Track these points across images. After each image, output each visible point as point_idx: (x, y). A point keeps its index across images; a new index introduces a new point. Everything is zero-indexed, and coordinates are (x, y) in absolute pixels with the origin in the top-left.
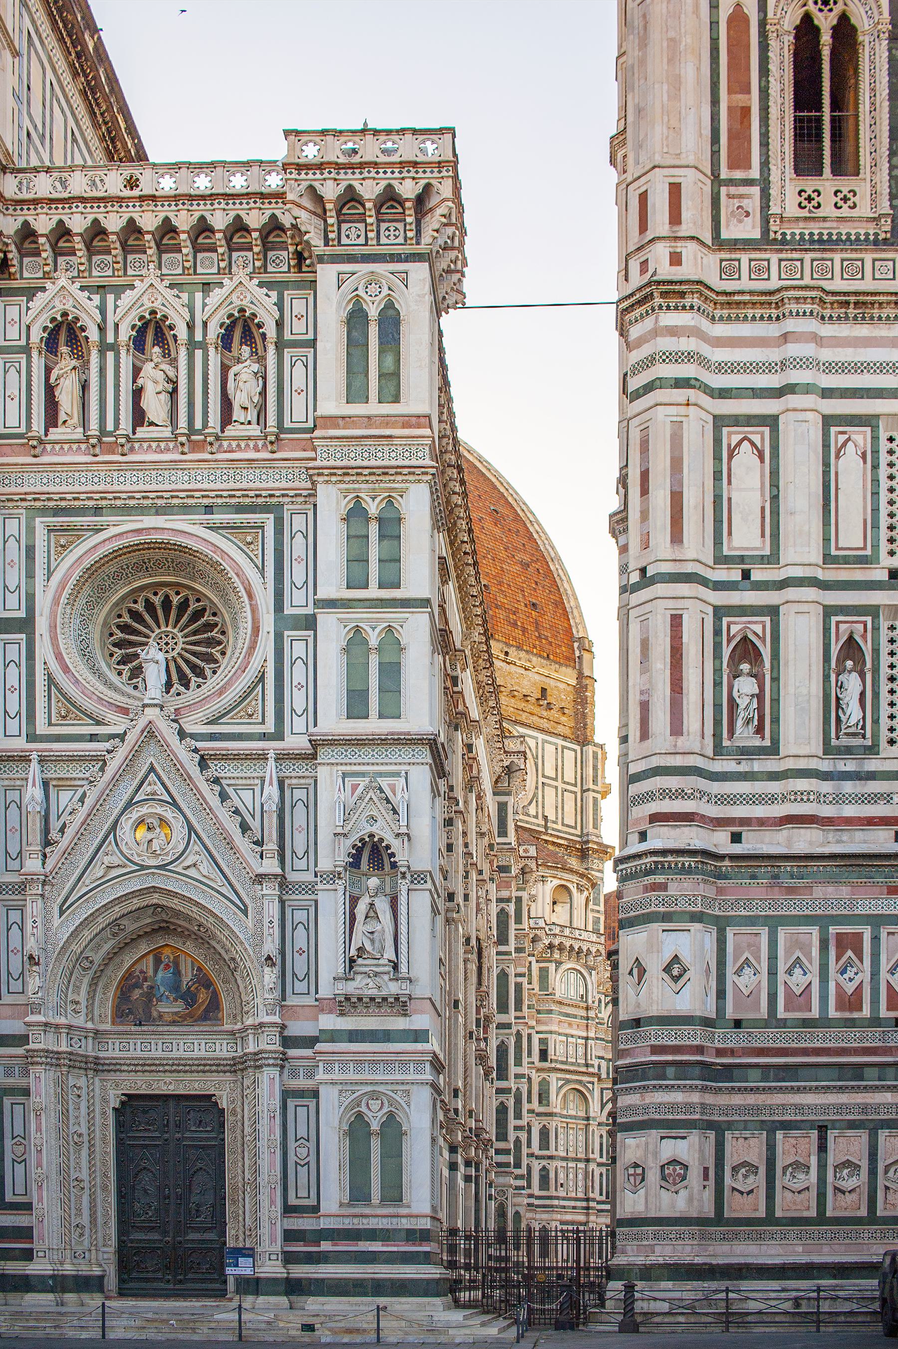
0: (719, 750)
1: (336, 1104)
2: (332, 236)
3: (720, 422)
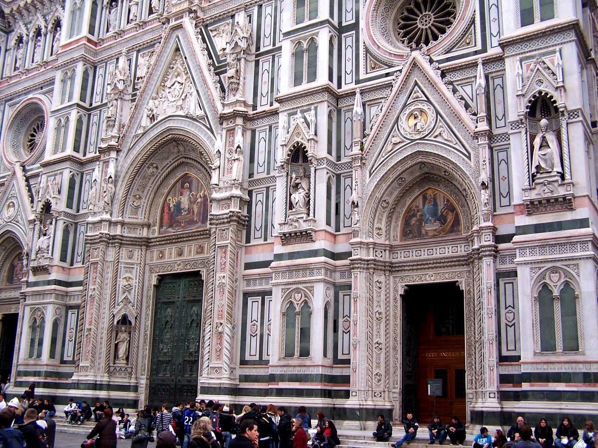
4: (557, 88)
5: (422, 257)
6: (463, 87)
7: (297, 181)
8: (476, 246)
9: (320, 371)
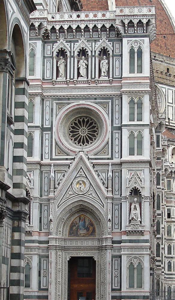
1: (126, 260)
2: (126, 32)
4: (142, 187)
5: (78, 245)
6: (102, 174)
9: (36, 294)
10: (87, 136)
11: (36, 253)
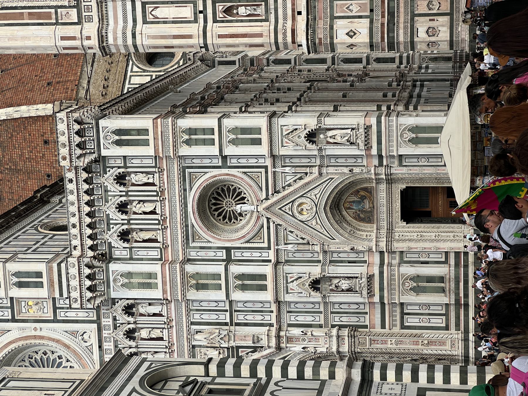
0: (266, 20)
1: (405, 149)
3: (145, 22)
7: (334, 286)
8: (384, 177)
9: (452, 268)
10: (236, 200)
11: (396, 269)
